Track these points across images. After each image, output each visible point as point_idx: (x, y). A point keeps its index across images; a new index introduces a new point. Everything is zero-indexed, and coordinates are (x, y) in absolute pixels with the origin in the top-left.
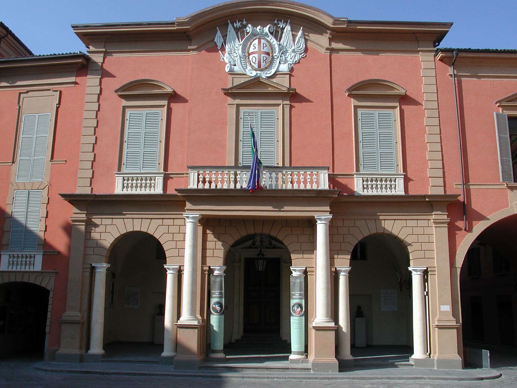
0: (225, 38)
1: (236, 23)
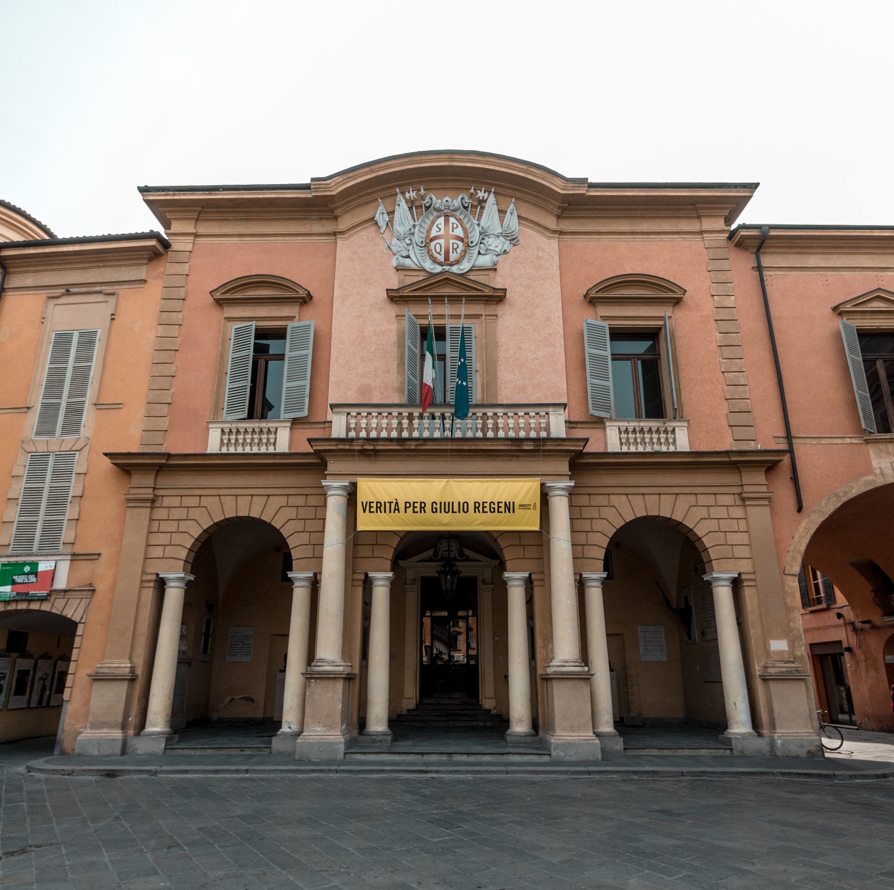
0: (391, 216)
1: (409, 193)
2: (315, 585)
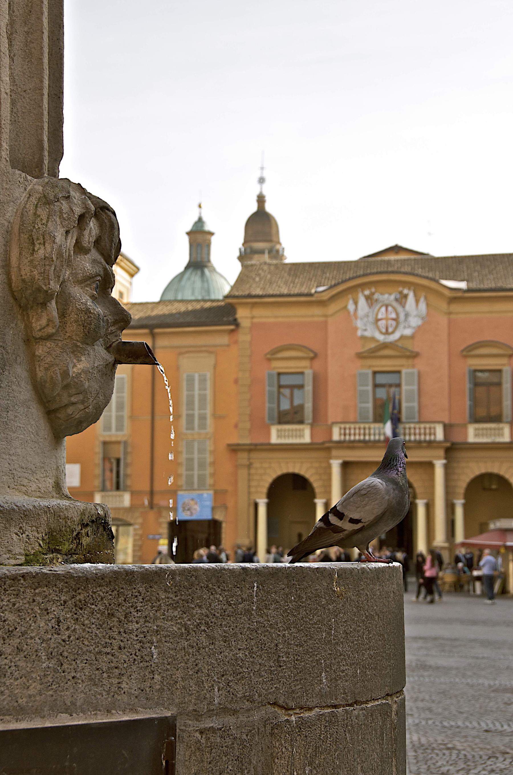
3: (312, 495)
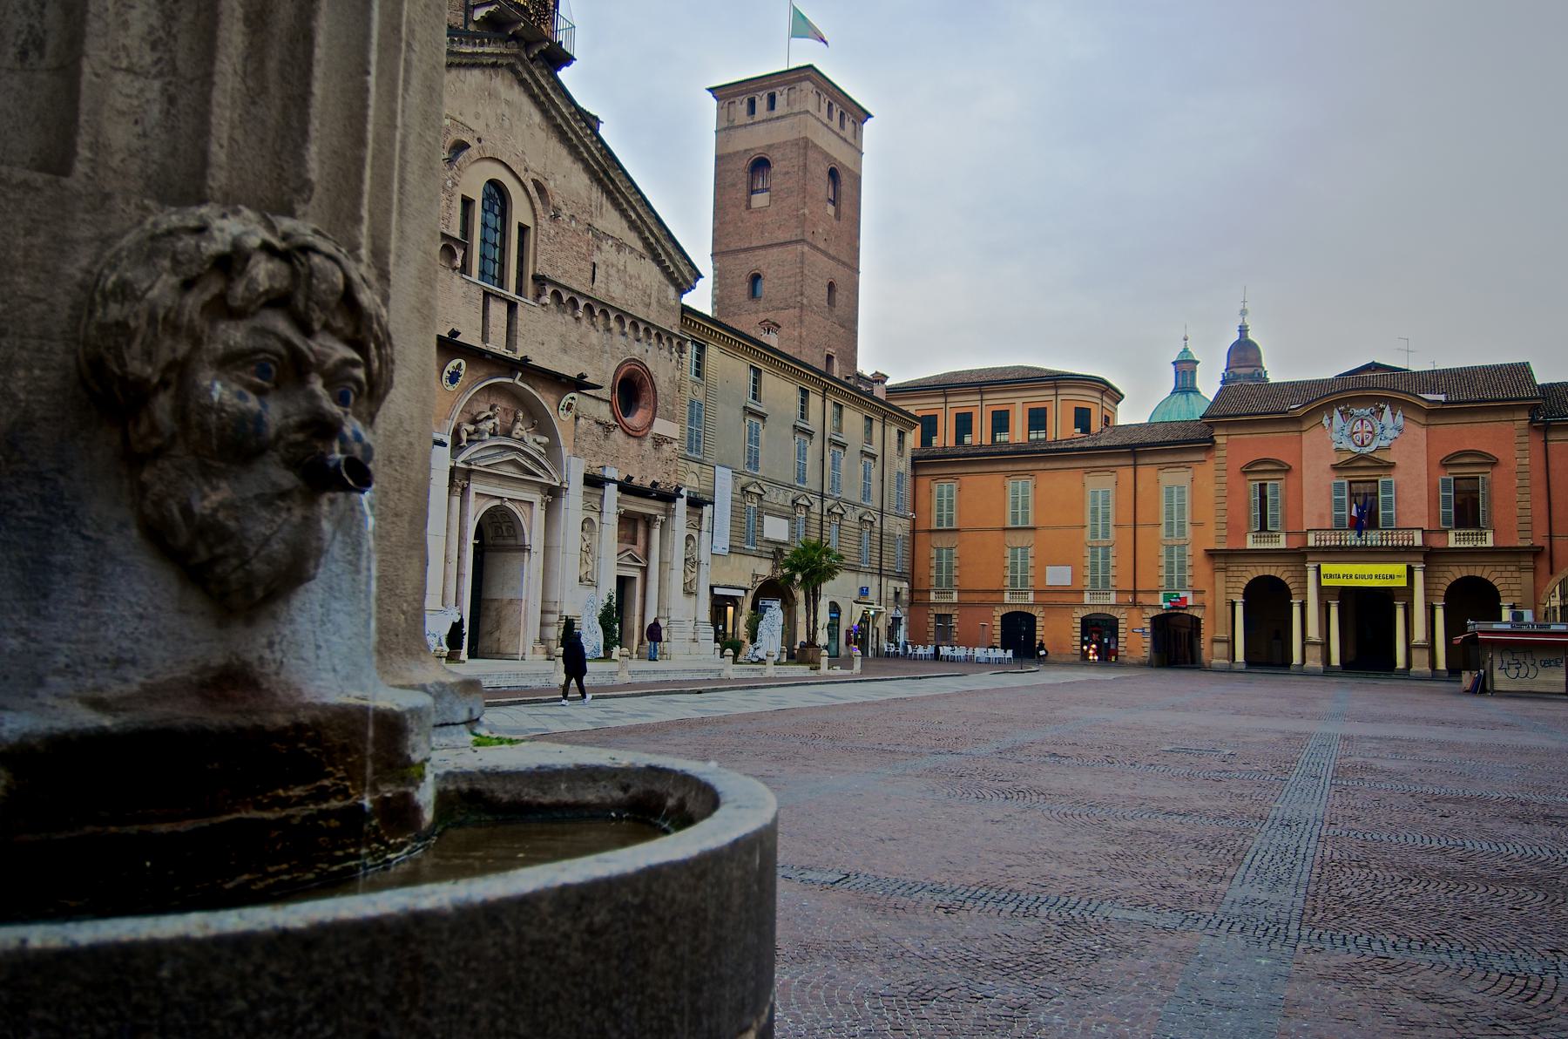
2: (1303, 606)
3: (1288, 595)
